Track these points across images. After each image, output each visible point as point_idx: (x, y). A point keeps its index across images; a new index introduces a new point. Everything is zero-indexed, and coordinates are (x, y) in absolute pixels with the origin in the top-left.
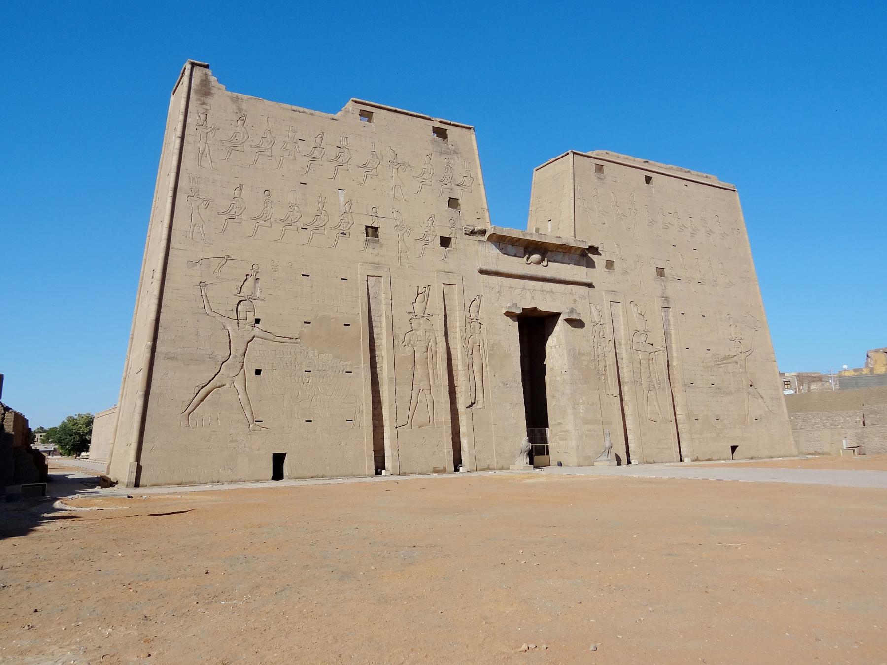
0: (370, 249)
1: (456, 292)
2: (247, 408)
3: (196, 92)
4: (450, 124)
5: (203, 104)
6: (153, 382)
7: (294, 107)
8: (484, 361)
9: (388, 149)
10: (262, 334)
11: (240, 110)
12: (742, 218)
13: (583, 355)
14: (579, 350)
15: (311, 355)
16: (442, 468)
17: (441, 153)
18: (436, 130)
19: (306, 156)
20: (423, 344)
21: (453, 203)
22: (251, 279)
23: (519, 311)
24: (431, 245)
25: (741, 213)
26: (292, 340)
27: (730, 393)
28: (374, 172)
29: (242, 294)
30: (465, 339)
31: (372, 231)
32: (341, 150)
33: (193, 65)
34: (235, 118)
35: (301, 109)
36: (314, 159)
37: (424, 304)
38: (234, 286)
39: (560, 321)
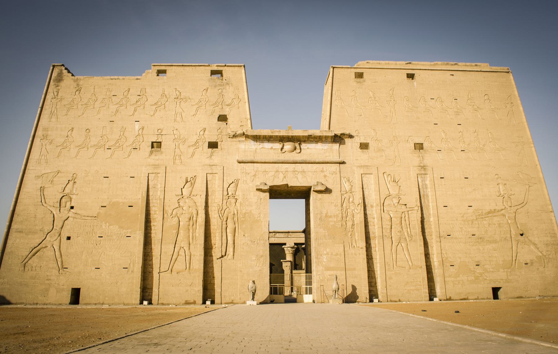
0: (153, 157)
1: (217, 178)
2: (59, 260)
3: (54, 81)
4: (225, 66)
5: (58, 86)
6: (8, 245)
7: (112, 77)
8: (237, 225)
9: (174, 90)
10: (73, 215)
11: (78, 85)
12: (516, 93)
13: (331, 217)
14: (326, 214)
15: (104, 227)
16: (192, 301)
17: (215, 86)
18: (213, 73)
19: (116, 104)
20: (187, 216)
21: (223, 118)
22: (71, 183)
23: (267, 188)
24: (201, 149)
25: (515, 89)
27: (495, 242)
28: (163, 106)
29: (65, 192)
30: (221, 211)
31: (156, 145)
32: (140, 97)
33: (54, 66)
34: (74, 91)
35: (116, 77)
36: (121, 105)
37: (191, 188)
38: (60, 188)
39: (312, 192)
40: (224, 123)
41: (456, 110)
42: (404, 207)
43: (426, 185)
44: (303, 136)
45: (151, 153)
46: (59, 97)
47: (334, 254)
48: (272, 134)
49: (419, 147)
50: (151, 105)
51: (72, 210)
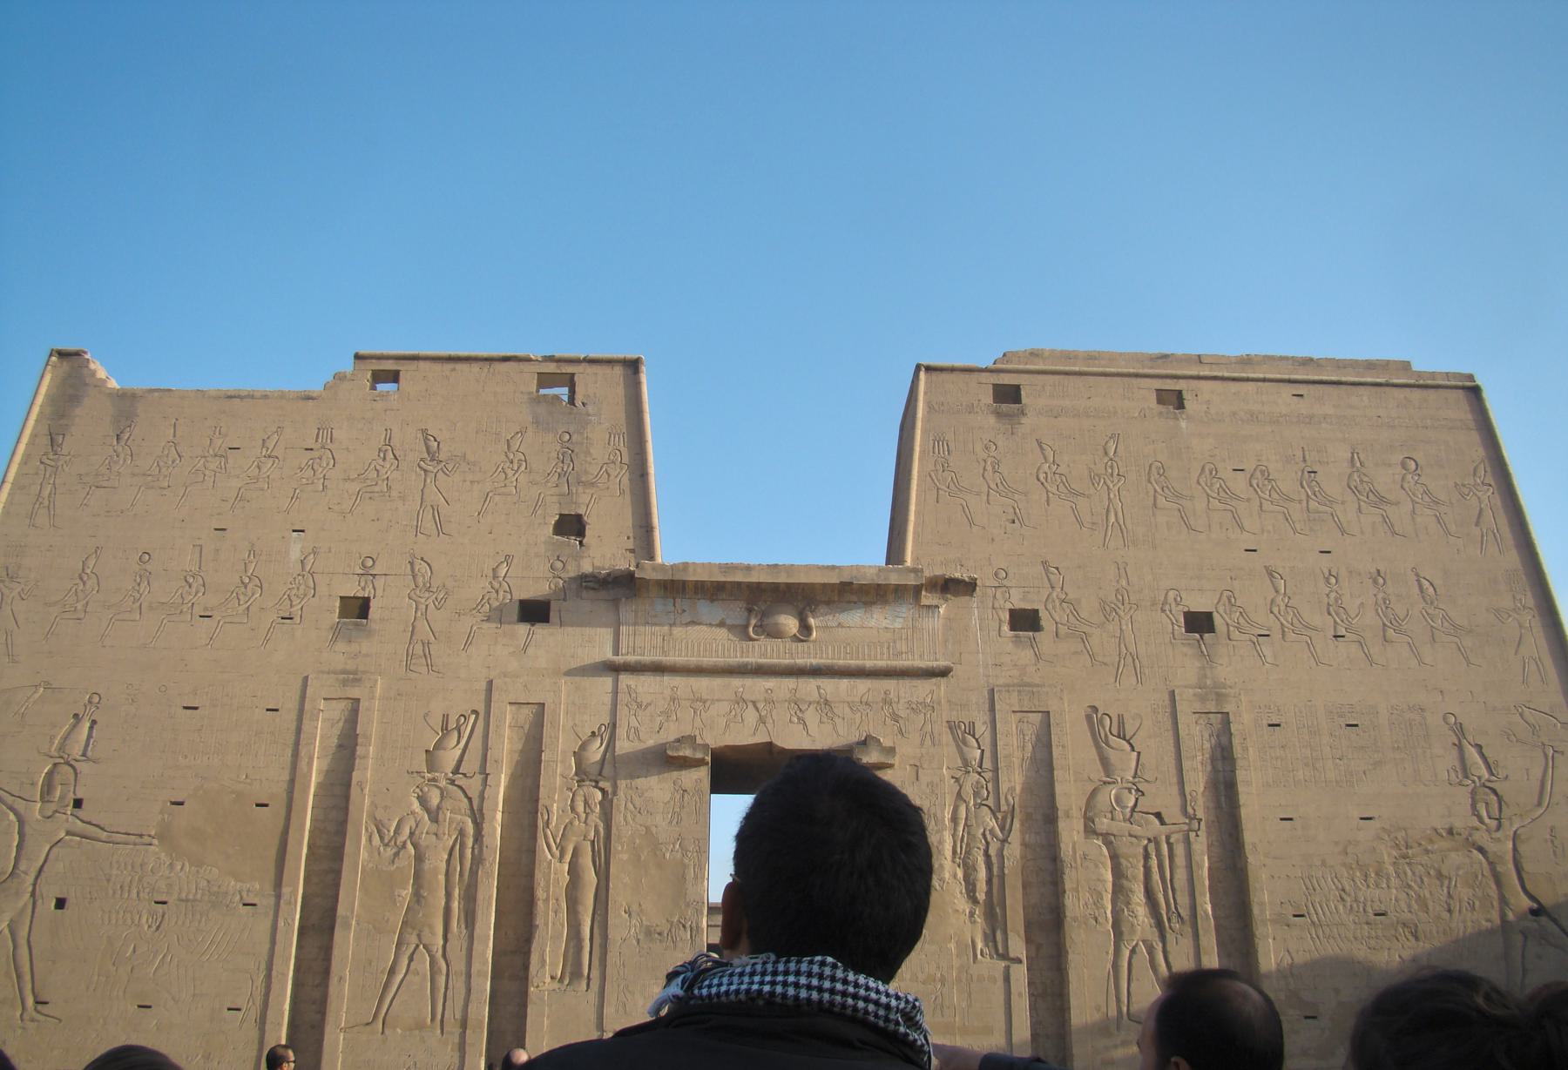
0: (341, 646)
5: (62, 416)
9: (420, 435)
18: (545, 380)
21: (571, 526)
23: (699, 755)
26: (138, 840)
31: (358, 608)
32: (315, 454)
37: (458, 752)
40: (574, 541)
41: (1313, 505)
44: (824, 585)
45: (337, 632)
46: (65, 451)
47: (921, 977)
48: (722, 579)
49: (1199, 623)
50: (347, 479)
51: (79, 812)
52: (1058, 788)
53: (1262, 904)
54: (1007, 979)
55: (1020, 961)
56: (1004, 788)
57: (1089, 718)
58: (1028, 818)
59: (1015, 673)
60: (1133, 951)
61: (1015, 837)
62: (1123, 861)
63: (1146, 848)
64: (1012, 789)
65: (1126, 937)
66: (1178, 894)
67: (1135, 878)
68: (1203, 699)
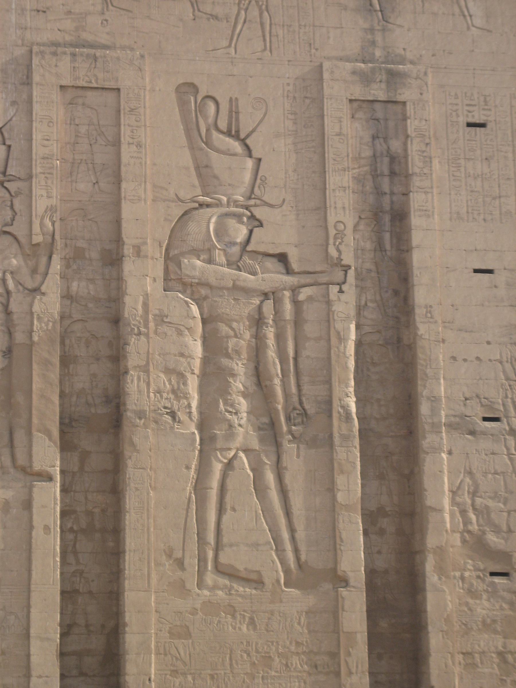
42: (271, 264)
43: (393, 159)
52: (127, 211)
53: (435, 400)
54: (28, 505)
55: (50, 478)
56: (40, 205)
57: (183, 104)
58: (76, 257)
59: (68, 24)
60: (229, 465)
61: (53, 287)
62: (224, 329)
63: (260, 308)
64: (52, 209)
65: (219, 444)
66: (305, 379)
67: (238, 352)
68: (367, 79)
